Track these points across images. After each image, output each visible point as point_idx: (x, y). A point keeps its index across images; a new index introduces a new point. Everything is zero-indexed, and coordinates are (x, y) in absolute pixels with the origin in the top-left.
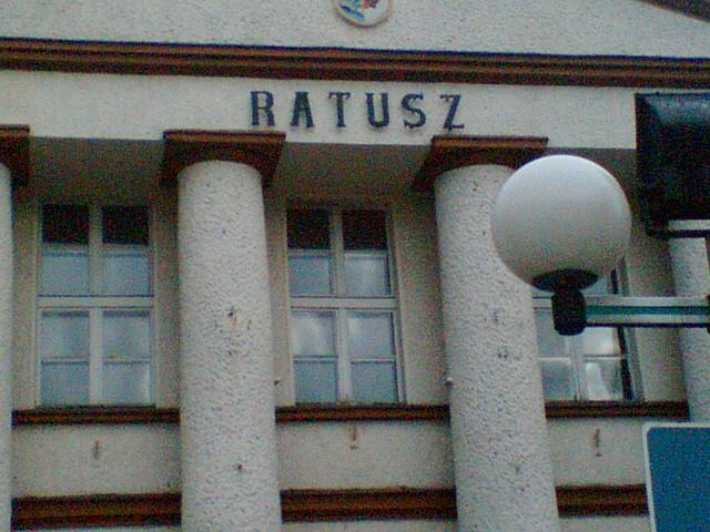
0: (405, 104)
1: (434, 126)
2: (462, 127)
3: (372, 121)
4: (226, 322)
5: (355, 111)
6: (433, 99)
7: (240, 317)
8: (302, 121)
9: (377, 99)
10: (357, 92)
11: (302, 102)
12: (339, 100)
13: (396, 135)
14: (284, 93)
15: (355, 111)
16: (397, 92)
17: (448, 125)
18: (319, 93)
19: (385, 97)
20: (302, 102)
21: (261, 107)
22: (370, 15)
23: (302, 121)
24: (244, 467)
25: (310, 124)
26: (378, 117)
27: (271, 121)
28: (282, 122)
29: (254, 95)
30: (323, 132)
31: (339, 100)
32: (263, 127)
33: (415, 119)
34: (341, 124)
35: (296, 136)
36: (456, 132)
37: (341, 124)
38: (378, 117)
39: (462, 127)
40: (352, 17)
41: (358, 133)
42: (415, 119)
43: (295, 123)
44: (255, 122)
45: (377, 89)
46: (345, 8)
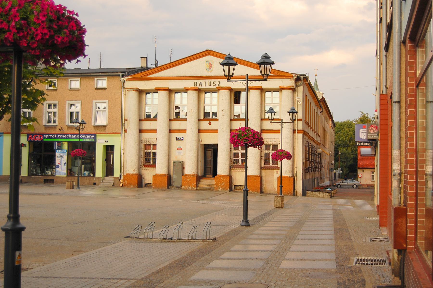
0: (213, 83)
1: (217, 86)
4: (191, 111)
10: (207, 81)
11: (201, 83)
12: (205, 82)
14: (198, 81)
16: (212, 81)
17: (219, 85)
18: (203, 81)
20: (201, 83)
21: (196, 84)
22: (210, 70)
31: (205, 82)
33: (214, 85)
34: (205, 86)
37: (205, 86)
42: (214, 85)
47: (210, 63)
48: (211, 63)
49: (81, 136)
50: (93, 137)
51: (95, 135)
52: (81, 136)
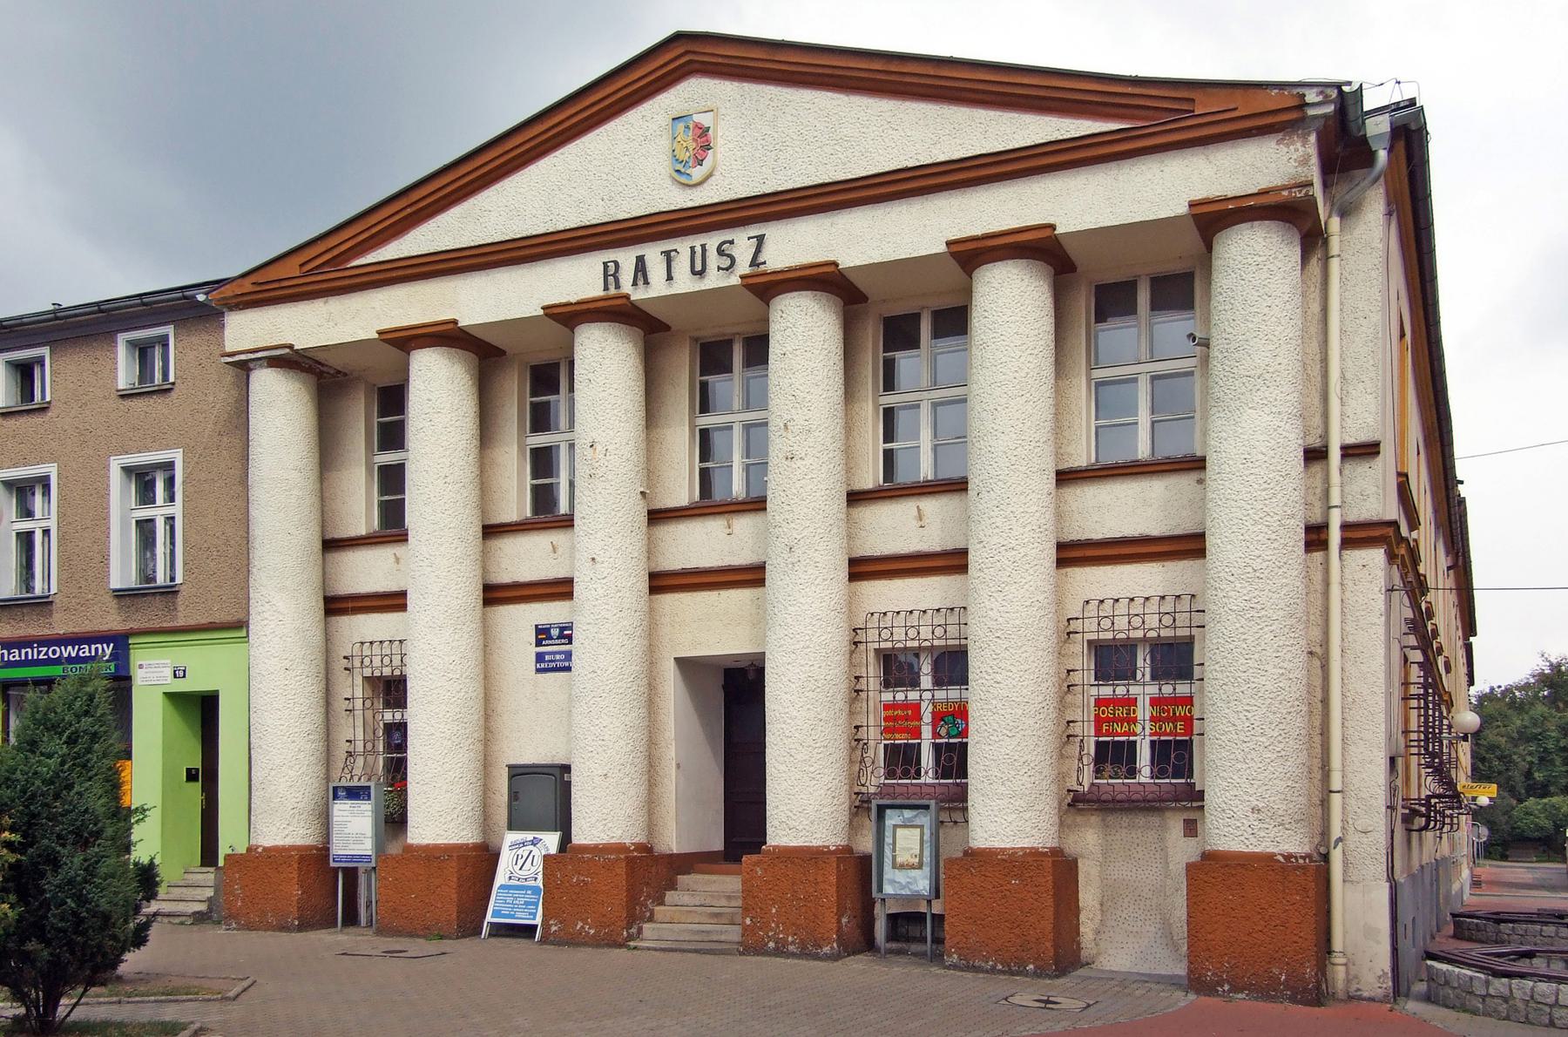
0: (720, 252)
1: (743, 267)
2: (765, 263)
3: (694, 272)
5: (682, 265)
6: (742, 242)
7: (598, 447)
8: (641, 282)
9: (698, 249)
10: (683, 246)
11: (641, 262)
13: (714, 280)
14: (626, 258)
15: (682, 265)
16: (713, 240)
18: (653, 253)
19: (703, 246)
20: (641, 262)
21: (611, 274)
22: (697, 173)
23: (641, 282)
24: (598, 559)
25: (646, 282)
26: (698, 267)
27: (618, 286)
28: (626, 286)
29: (605, 264)
30: (658, 287)
31: (668, 256)
32: (612, 291)
33: (726, 262)
34: (670, 278)
35: (638, 295)
36: (762, 267)
37: (670, 278)
38: (698, 267)
39: (765, 263)
40: (683, 179)
41: (684, 283)
42: (726, 262)
43: (635, 284)
44: (606, 288)
45: (697, 241)
46: (678, 171)
47: (698, 126)
48: (705, 120)
49: (54, 652)
50: (108, 652)
51: (121, 642)
52: (54, 652)
